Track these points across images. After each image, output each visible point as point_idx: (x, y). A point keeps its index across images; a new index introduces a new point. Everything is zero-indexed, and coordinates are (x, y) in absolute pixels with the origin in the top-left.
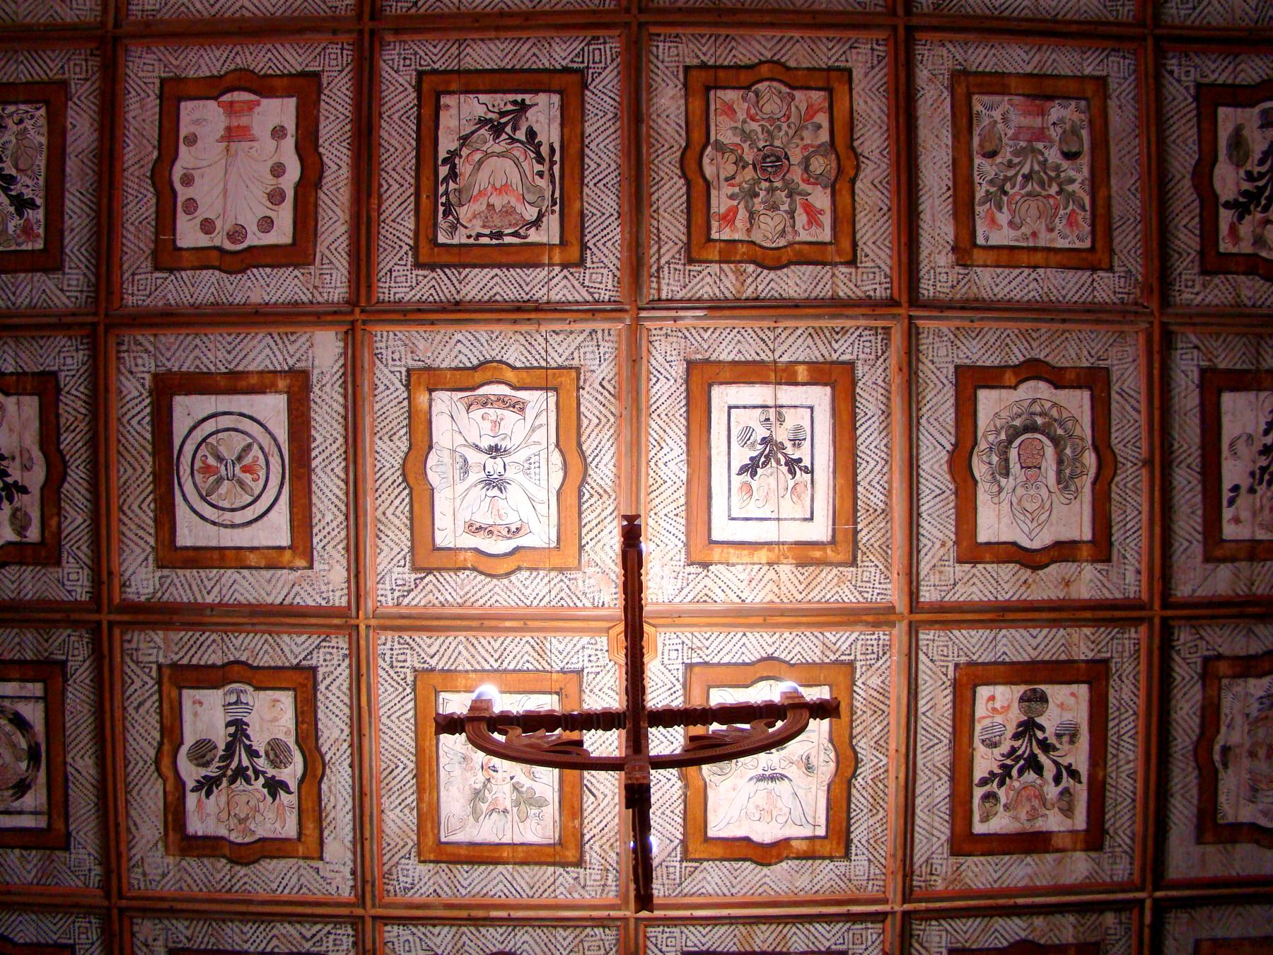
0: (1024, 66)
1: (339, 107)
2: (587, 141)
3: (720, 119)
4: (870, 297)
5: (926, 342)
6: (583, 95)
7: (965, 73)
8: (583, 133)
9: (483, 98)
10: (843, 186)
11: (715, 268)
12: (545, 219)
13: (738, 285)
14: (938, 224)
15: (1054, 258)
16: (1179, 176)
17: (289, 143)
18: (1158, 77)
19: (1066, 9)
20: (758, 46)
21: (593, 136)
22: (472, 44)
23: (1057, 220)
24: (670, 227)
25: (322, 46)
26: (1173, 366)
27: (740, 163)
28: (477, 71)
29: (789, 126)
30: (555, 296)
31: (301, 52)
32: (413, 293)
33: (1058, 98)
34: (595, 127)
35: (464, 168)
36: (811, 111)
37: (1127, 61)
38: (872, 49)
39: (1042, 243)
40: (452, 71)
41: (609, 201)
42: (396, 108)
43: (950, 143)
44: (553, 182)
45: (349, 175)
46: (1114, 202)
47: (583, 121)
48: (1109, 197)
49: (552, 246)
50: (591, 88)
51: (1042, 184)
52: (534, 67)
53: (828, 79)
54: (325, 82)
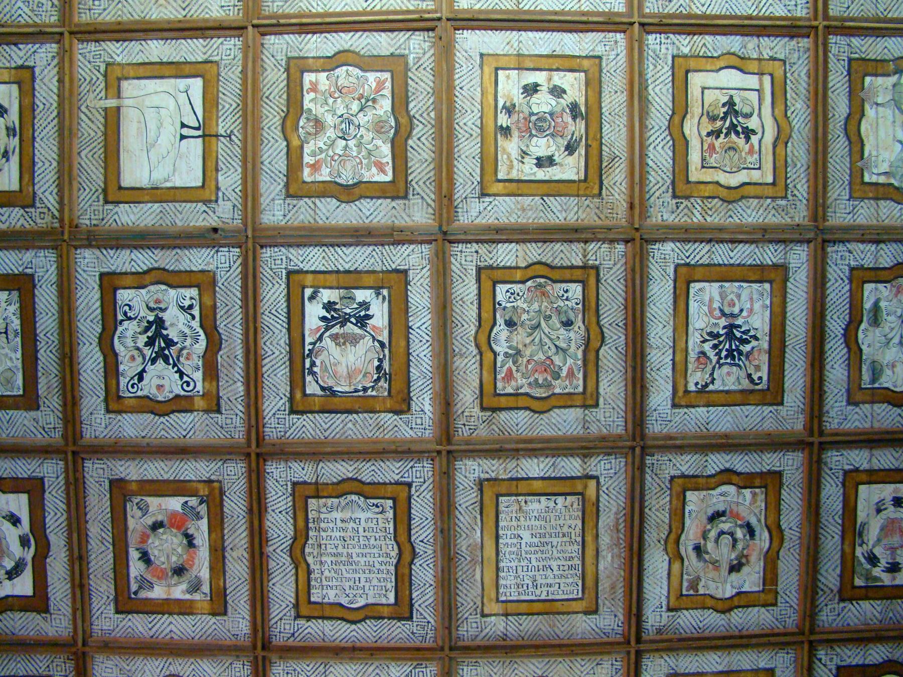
25: (230, 662)
31: (215, 665)
37: (789, 656)
38: (612, 665)
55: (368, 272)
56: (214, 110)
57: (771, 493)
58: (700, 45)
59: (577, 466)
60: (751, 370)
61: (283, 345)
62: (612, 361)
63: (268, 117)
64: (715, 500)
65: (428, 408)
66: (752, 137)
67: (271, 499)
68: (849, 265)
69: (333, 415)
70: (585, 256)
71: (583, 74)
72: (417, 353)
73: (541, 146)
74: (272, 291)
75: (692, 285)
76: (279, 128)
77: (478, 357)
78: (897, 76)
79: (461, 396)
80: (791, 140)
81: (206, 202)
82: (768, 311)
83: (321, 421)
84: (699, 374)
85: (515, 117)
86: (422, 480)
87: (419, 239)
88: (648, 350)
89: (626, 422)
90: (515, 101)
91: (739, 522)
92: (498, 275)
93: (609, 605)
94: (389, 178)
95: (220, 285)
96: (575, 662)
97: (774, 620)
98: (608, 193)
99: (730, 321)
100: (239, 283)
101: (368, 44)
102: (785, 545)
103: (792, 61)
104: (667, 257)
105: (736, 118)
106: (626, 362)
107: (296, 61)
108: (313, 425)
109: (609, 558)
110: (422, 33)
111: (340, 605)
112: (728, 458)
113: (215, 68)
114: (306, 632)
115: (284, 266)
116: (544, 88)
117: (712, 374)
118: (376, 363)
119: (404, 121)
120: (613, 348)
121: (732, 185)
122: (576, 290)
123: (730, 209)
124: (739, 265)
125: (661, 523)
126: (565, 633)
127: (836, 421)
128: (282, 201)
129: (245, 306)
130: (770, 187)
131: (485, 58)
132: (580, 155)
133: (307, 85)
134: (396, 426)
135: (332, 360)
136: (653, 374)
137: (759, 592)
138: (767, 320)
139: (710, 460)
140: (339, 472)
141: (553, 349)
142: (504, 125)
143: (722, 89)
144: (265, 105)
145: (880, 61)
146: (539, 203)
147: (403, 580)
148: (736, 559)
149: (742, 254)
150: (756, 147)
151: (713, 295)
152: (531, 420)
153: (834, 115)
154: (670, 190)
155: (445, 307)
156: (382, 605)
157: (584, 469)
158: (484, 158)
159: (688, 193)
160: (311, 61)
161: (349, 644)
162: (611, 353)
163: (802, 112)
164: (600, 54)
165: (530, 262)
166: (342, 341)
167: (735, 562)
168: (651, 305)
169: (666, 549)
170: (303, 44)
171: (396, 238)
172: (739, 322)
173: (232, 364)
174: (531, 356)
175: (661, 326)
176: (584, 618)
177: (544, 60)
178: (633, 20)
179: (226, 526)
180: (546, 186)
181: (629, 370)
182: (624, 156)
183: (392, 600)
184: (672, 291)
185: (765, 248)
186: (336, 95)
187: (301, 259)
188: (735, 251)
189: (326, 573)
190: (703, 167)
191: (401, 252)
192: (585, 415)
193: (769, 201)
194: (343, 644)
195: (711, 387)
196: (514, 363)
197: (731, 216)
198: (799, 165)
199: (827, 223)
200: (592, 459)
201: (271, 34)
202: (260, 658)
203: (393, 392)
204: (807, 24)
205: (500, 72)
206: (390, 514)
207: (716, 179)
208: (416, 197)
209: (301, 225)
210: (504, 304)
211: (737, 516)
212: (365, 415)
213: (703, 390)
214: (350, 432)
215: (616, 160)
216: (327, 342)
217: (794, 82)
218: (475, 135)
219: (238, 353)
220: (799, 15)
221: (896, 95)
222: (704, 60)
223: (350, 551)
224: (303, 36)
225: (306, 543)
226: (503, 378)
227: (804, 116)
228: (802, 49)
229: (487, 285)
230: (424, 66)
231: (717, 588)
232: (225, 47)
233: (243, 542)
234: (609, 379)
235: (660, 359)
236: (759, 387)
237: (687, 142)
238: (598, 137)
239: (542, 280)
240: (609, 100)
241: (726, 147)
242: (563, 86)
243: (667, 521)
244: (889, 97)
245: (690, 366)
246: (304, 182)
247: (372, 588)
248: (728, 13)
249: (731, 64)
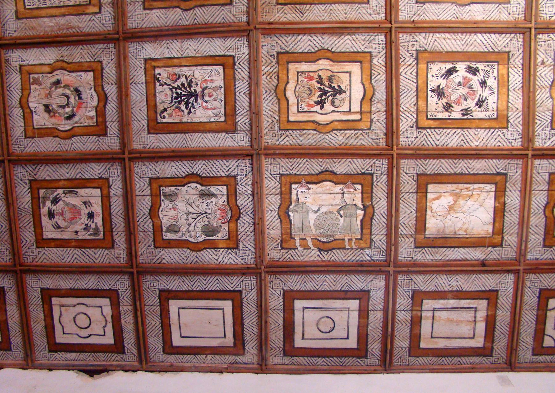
19: (13, 121)
57: (93, 129)
58: (379, 71)
62: (173, 17)
64: (88, 91)
66: (319, 106)
68: (238, 175)
75: (222, 67)
78: (362, 207)
82: (207, 121)
84: (166, 75)
88: (180, 41)
89: (135, 29)
91: (75, 109)
93: (22, 27)
97: (16, 137)
98: (279, 9)
102: (62, 141)
103: (370, 134)
104: (239, 50)
105: (331, 95)
109: (51, 24)
117: (166, 84)
120: (180, 17)
121: (287, 92)
123: (271, 91)
124: (235, 99)
125: (73, 57)
127: (139, 171)
130: (287, 119)
136: (165, 45)
137: (33, 126)
138: (201, 120)
139: (113, 86)
145: (372, 196)
148: (53, 109)
149: (242, 101)
150: (312, 109)
151: (216, 82)
153: (335, 163)
154: (282, 51)
157: (105, 4)
159: (281, 63)
162: (177, 16)
163: (337, 141)
164: (371, 3)
167: (51, 108)
168: (208, 41)
169: (57, 61)
172: (199, 101)
175: (195, 48)
176: (13, 11)
178: (393, 23)
184: (218, 54)
185: (247, 117)
188: (244, 96)
190: (298, 72)
192: (138, 2)
193: (277, 118)
195: (158, 84)
198: (301, 139)
199: (263, 157)
200: (111, 9)
204: (394, 143)
207: (291, 81)
211: (79, 107)
215: (301, 14)
217: (356, 136)
220: (401, 139)
221: (349, 206)
222: (369, 74)
227: (334, 142)
228: (378, 141)
231: (34, 97)
234: (161, 16)
235: (174, 49)
236: (159, 117)
237: (314, 62)
238: (316, 2)
240: (340, 9)
241: (312, 89)
243: (75, 61)
244: (348, 202)
248: (401, 90)
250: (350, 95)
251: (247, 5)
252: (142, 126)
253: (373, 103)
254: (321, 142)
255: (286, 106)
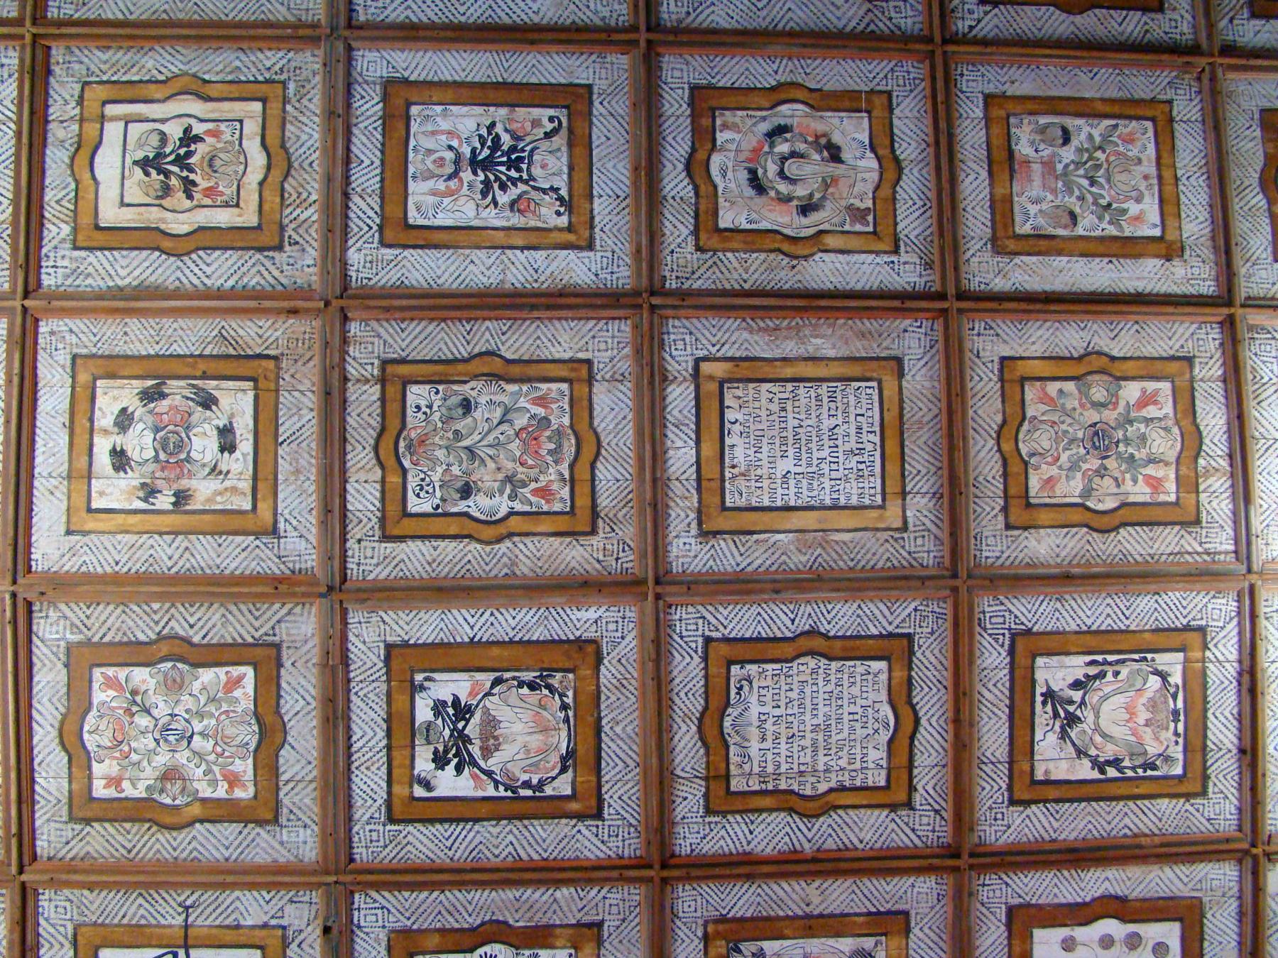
0: (981, 178)
1: (1045, 884)
2: (1085, 628)
3: (1058, 493)
4: (1221, 344)
5: (1256, 291)
6: (1038, 634)
7: (994, 239)
8: (1076, 633)
9: (1038, 735)
10: (1119, 369)
11: (1203, 497)
12: (1160, 668)
13: (1218, 474)
14: (1146, 274)
15: (1166, 160)
16: (1072, 28)
17: (1080, 933)
18: (976, 42)
20: (982, 454)
21: (1079, 622)
22: (982, 750)
23: (1130, 154)
24: (1166, 542)
25: (979, 906)
26: (1251, 45)
27: (1101, 472)
28: (1011, 744)
29: (1063, 422)
30: (1233, 654)
31: (985, 928)
32: (1230, 796)
33: (1010, 146)
34: (1070, 620)
35: (1109, 751)
36: (1045, 399)
37: (965, 72)
38: (979, 335)
39: (1153, 171)
40: (1010, 770)
41: (1143, 605)
42: (1047, 825)
43: (1066, 259)
44: (1123, 661)
45: (1114, 868)
46: (1107, 95)
47: (1064, 633)
48: (1103, 100)
49: (1186, 660)
50: (1030, 625)
51: (1098, 167)
52: (1007, 685)
53: (1012, 381)
54: (1017, 901)
55: (389, 703)
56: (148, 930)
57: (723, 102)
58: (59, 208)
59: (678, 391)
60: (540, 133)
61: (498, 829)
62: (522, 340)
63: (158, 851)
64: (732, 185)
65: (592, 614)
66: (194, 132)
67: (732, 846)
69: (603, 754)
70: (367, 381)
71: (99, 383)
72: (509, 630)
73: (204, 445)
74: (418, 845)
75: (411, 221)
76: (175, 834)
77: (516, 539)
79: (574, 564)
80: (200, 75)
81: (285, 944)
82: (452, 107)
83: (613, 773)
84: (544, 210)
85: (160, 484)
86: (700, 621)
87: (338, 626)
88: (508, 286)
89: (614, 319)
90: (136, 483)
91: (766, 149)
92: (393, 510)
93: (889, 341)
94: (249, 671)
95: (409, 923)
96: (975, 390)
98: (274, 346)
99: (465, 164)
100: (406, 894)
101: (50, 700)
102: (800, 80)
103: (84, 72)
104: (369, 258)
105: (166, 156)
106: (525, 320)
107: (75, 810)
108: (619, 784)
109: (819, 341)
110: (35, 621)
111: (890, 742)
112: (669, 166)
113: (84, 929)
114: (932, 792)
115: (381, 828)
116: (119, 440)
117: (544, 191)
118: (525, 690)
119: (164, 649)
120: (504, 338)
121: (265, 162)
122: (417, 394)
123: (300, 165)
124: (382, 152)
125: (765, 265)
126: (930, 405)
127: (616, 7)
128: (284, 831)
129: (441, 886)
130: (268, 105)
131: (73, 528)
132: (217, 388)
133: (111, 793)
134: (619, 661)
135: (523, 756)
136: (542, 278)
137: (870, 118)
138: (466, 109)
139: (672, 194)
140: (690, 745)
141: (504, 427)
142: (173, 499)
143: (123, 177)
144: (140, 855)
146: (287, 449)
147: (853, 649)
148: (821, 152)
149: (366, 147)
150: (210, 126)
151: (426, 190)
152: (610, 459)
153: (165, 11)
154: (271, 254)
155: (440, 589)
156: (890, 679)
157: (685, 380)
158: (221, 530)
159: (275, 228)
160: (74, 786)
161: (950, 728)
163: (159, 58)
164: (69, 357)
165: (374, 461)
166: (492, 741)
167: (826, 154)
168: (439, 282)
169: (806, 257)
170: (50, 798)
171: (338, 660)
172: (466, 151)
173: (527, 905)
174: (514, 460)
175: (472, 267)
176: (908, 377)
177: (77, 440)
178: (19, 308)
179: (772, 913)
180: (262, 440)
181: (536, 314)
182: (218, 322)
183: (883, 665)
184: (420, 251)
185: (358, 113)
186: (126, 749)
187: (370, 802)
188: (363, 157)
189: (843, 763)
190: (237, 205)
191: (359, 654)
192: (604, 379)
193: (288, 108)
194: (950, 737)
195: (564, 193)
196: (524, 485)
197: (311, 164)
198: (238, 63)
199: (323, 22)
200: (670, 368)
201: (34, 846)
202: (972, 861)
203: (567, 665)
204: (28, 50)
205: (94, 505)
206: (753, 669)
207: (255, 186)
208: (277, 631)
209: (318, 802)
210: (437, 501)
211: (756, 151)
212: (603, 707)
213: (568, 205)
214: (629, 729)
216: (493, 763)
218: (186, 544)
219: (511, 896)
220: (16, 61)
222: (80, 203)
223: (809, 728)
224: (37, 797)
225: (798, 794)
226: (548, 502)
229: (408, 526)
230: (83, 617)
231: (864, 180)
232: (53, 915)
233: (797, 887)
234: (549, 344)
235: (521, 268)
237: (201, 229)
238: (190, 360)
239: (402, 444)
240: (138, 344)
241: (207, 169)
242: (116, 412)
243: (763, 256)
245: (532, 223)
246: (255, 797)
247: (865, 695)
248: (12, 166)
249: (87, 162)
250: (124, 156)
251: (348, 358)
252: (605, 103)
253: (76, 139)
254: (193, 55)
255: (267, 132)
